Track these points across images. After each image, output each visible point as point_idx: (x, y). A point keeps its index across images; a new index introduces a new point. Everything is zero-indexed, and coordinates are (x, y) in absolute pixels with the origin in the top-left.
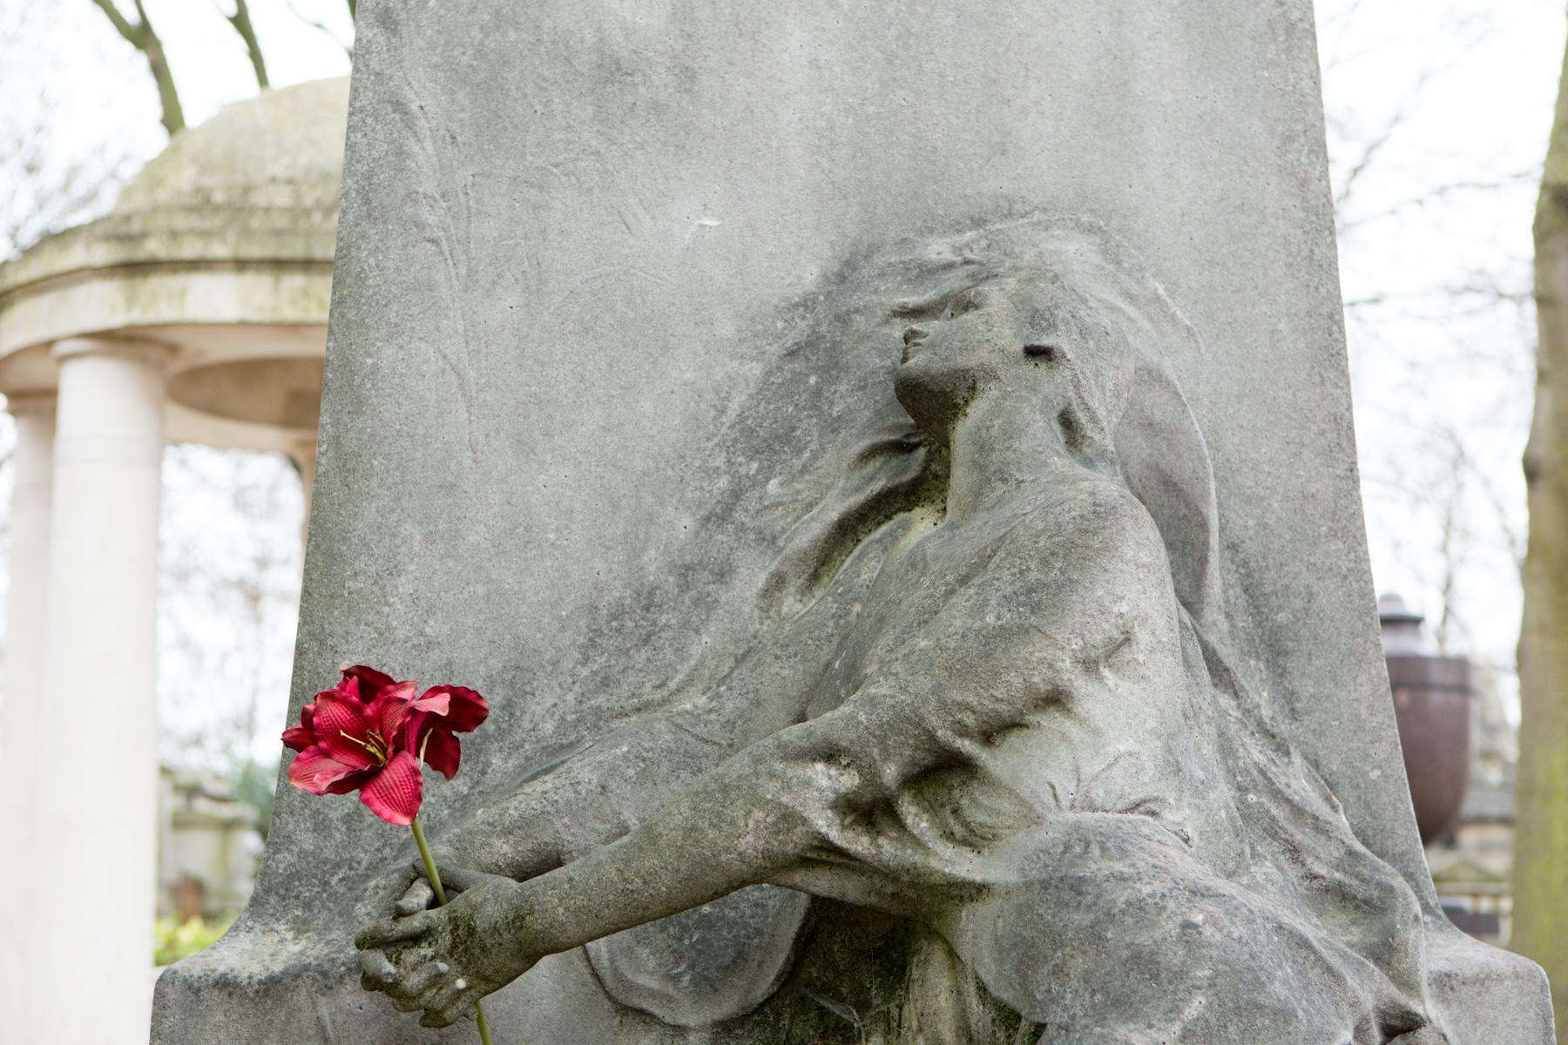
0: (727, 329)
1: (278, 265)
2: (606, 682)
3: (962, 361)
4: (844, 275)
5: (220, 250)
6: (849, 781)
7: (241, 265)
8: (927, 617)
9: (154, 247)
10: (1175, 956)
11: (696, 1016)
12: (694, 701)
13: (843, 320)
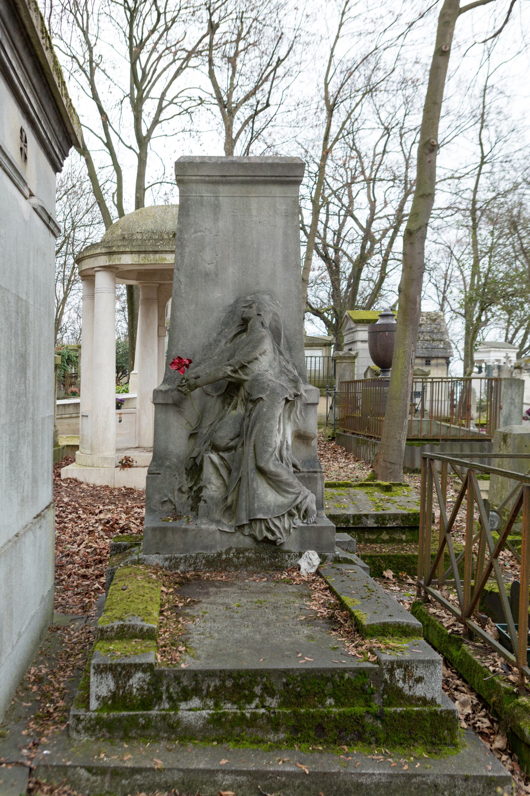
0: (221, 309)
1: (139, 252)
2: (205, 355)
3: (250, 316)
4: (237, 302)
5: (128, 250)
6: (232, 368)
7: (132, 252)
8: (243, 349)
9: (114, 249)
10: (266, 387)
11: (215, 395)
12: (216, 358)
13: (236, 308)
